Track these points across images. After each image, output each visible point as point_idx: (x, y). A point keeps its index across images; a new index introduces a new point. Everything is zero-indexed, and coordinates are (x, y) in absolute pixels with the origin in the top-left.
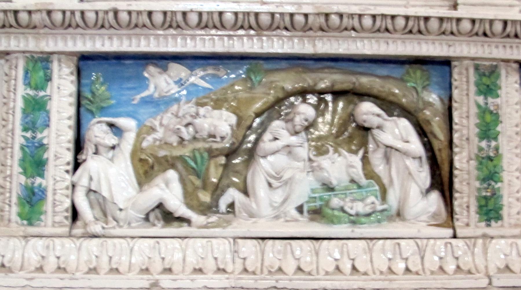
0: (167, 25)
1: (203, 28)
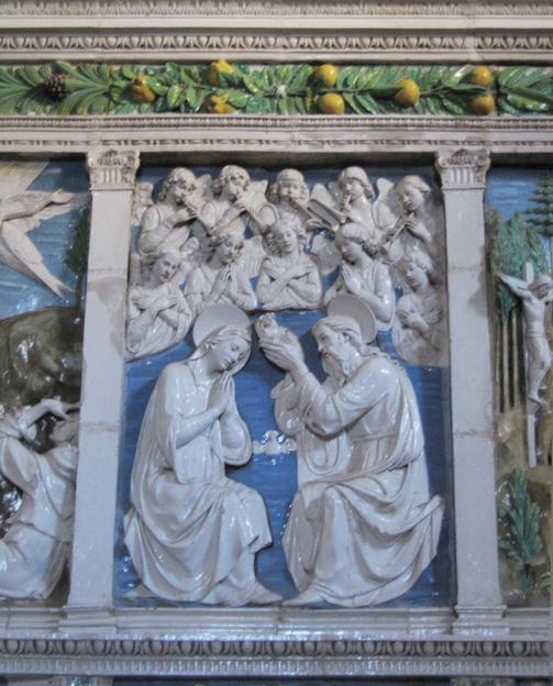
0: (195, 651)
1: (225, 655)
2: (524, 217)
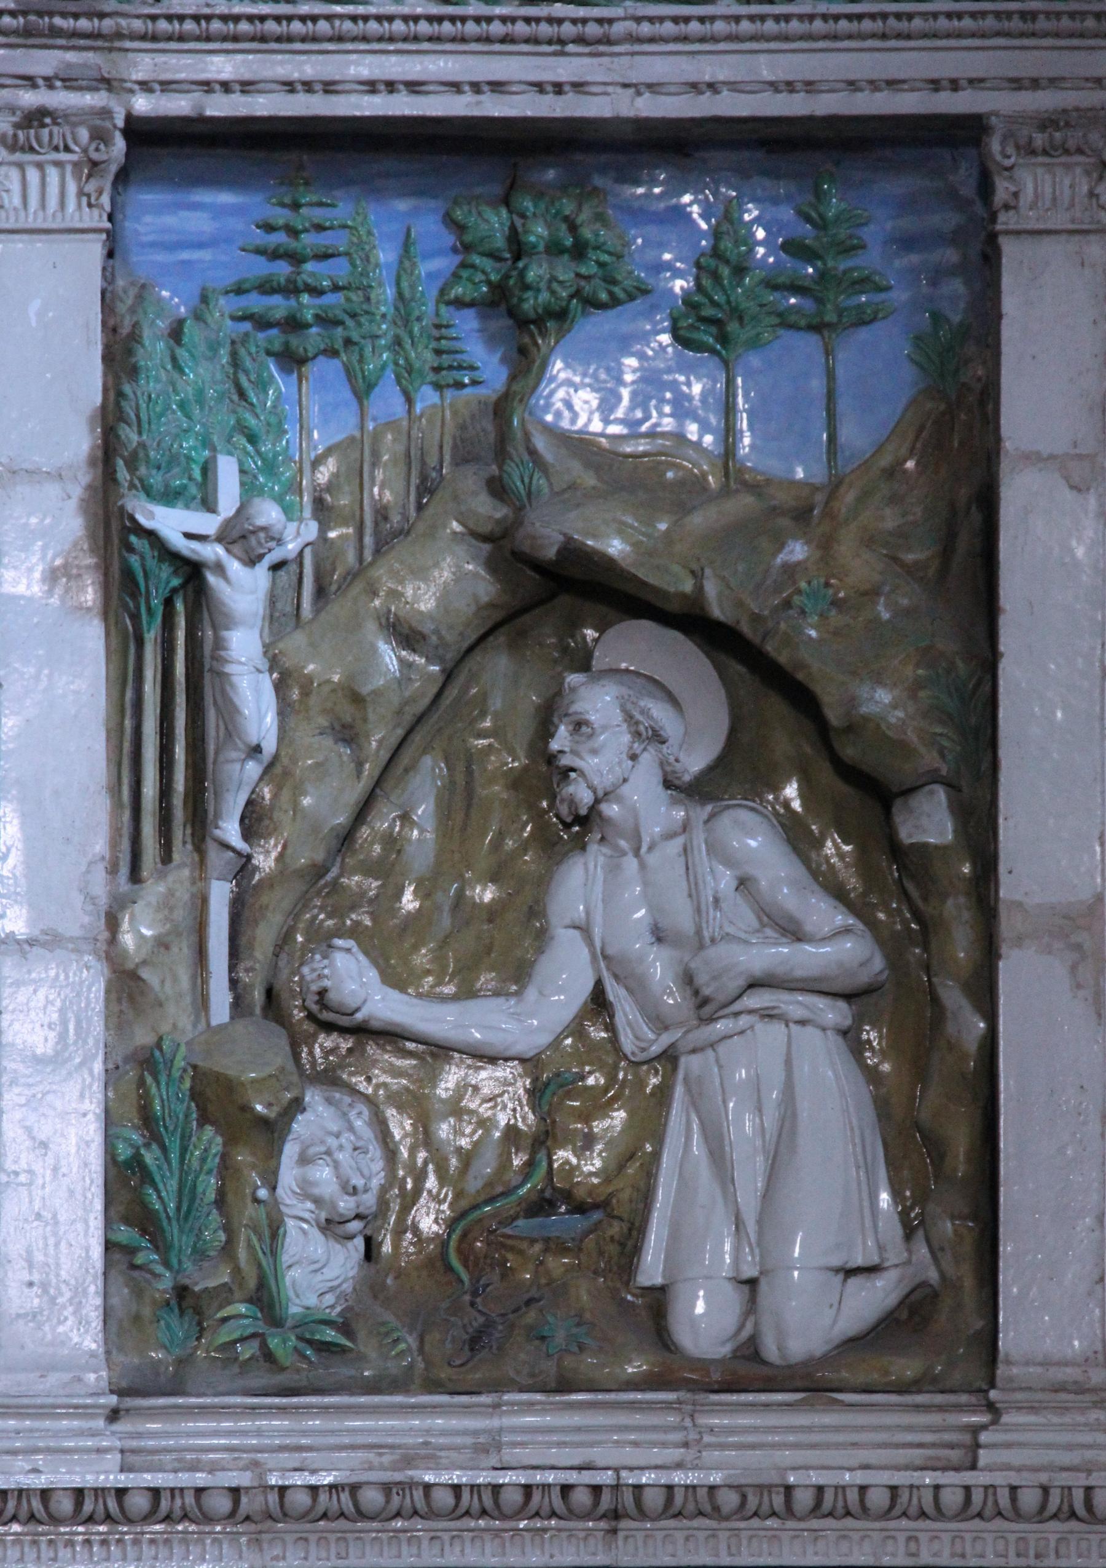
2: (225, 305)
